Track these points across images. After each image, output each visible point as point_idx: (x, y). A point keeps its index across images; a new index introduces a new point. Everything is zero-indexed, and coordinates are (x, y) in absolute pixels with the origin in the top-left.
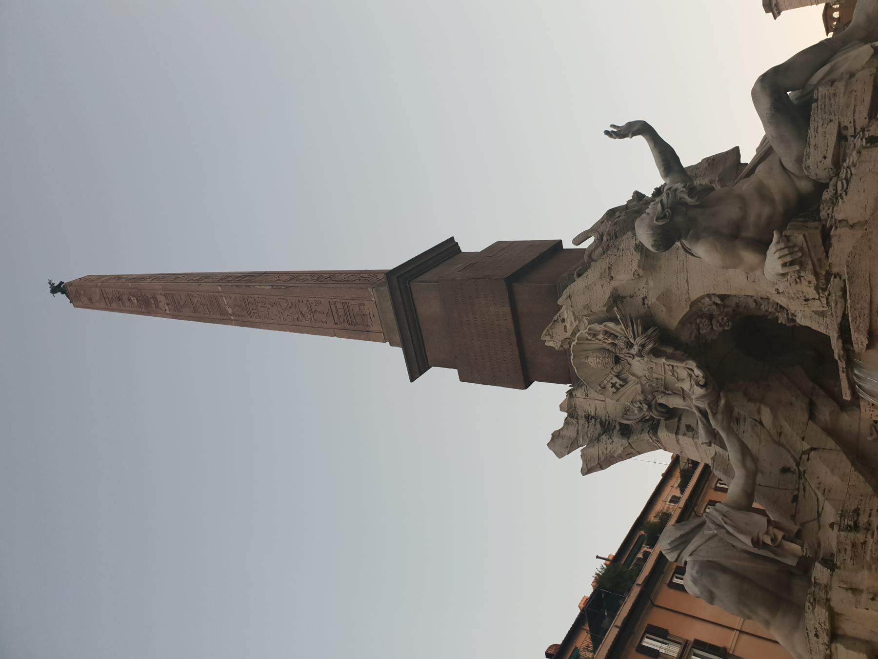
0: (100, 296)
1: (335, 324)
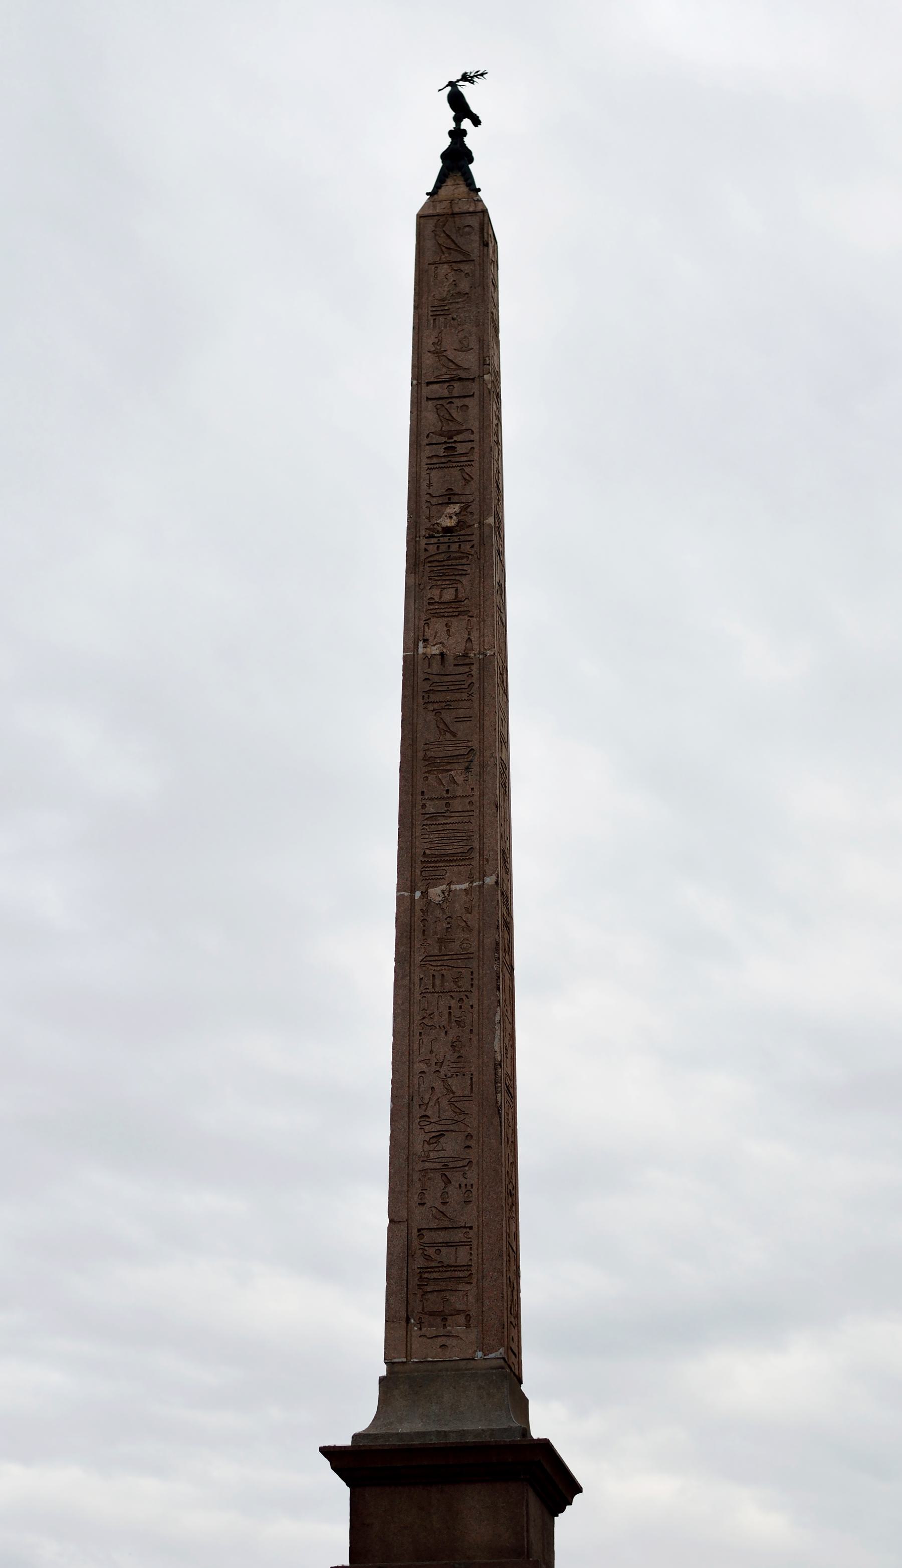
1: (419, 1230)
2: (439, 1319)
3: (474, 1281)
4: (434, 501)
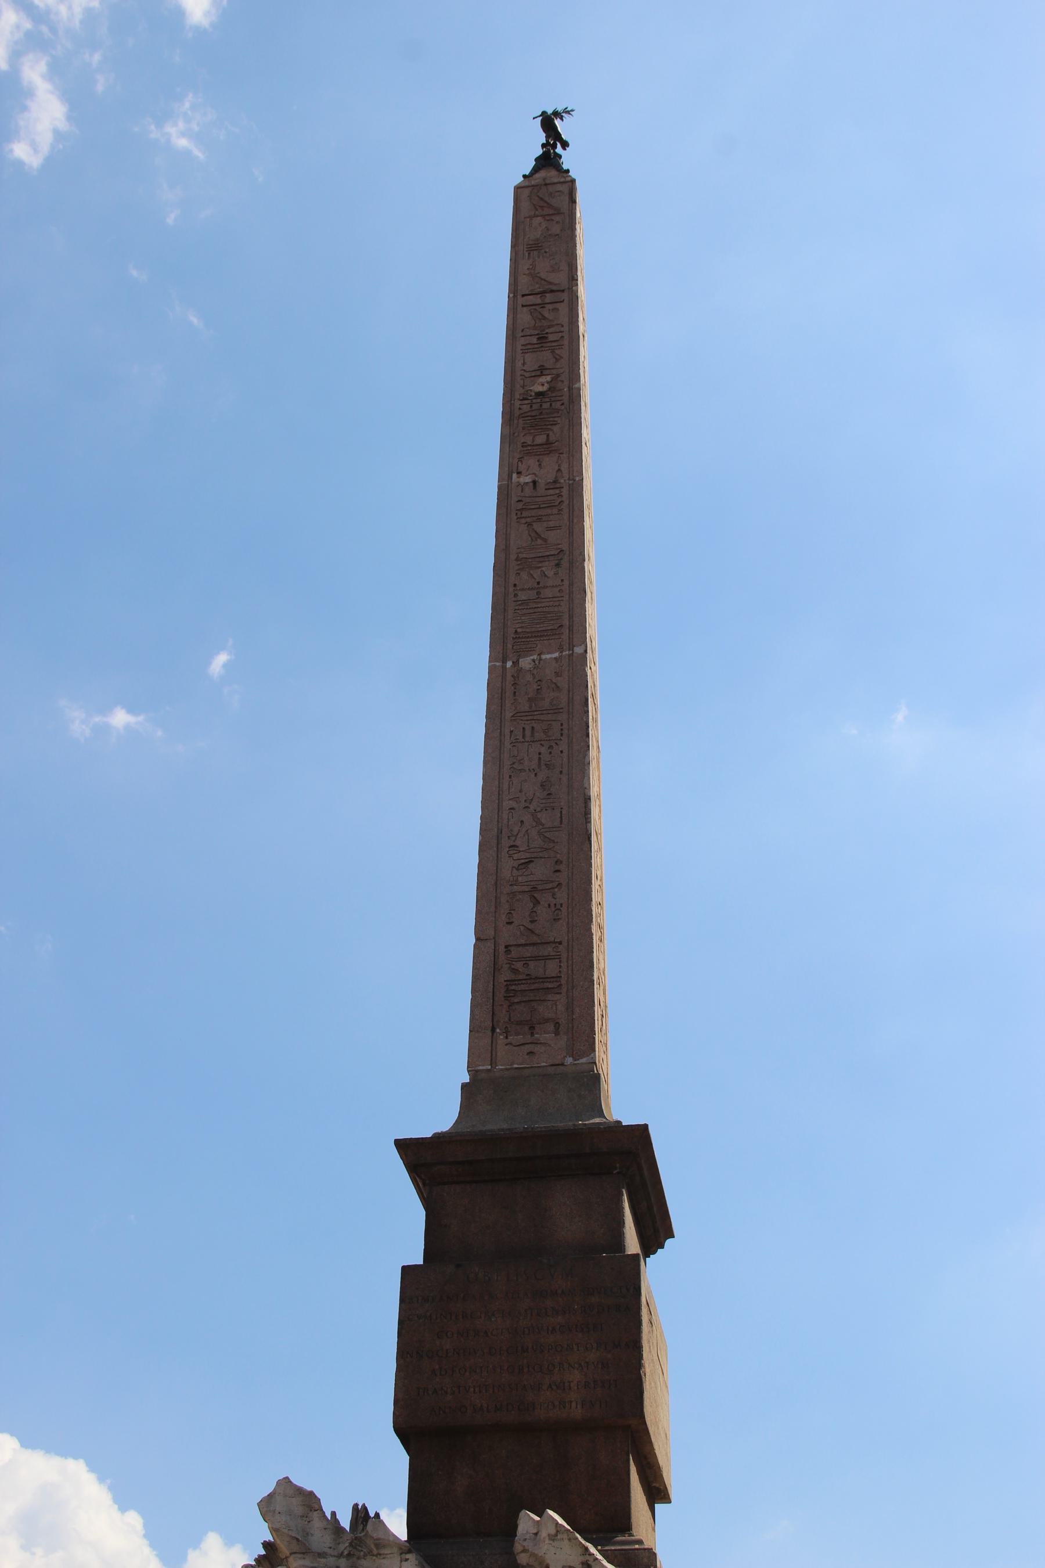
0: (550, 283)
1: (506, 947)
2: (526, 1028)
3: (564, 990)
4: (527, 375)
